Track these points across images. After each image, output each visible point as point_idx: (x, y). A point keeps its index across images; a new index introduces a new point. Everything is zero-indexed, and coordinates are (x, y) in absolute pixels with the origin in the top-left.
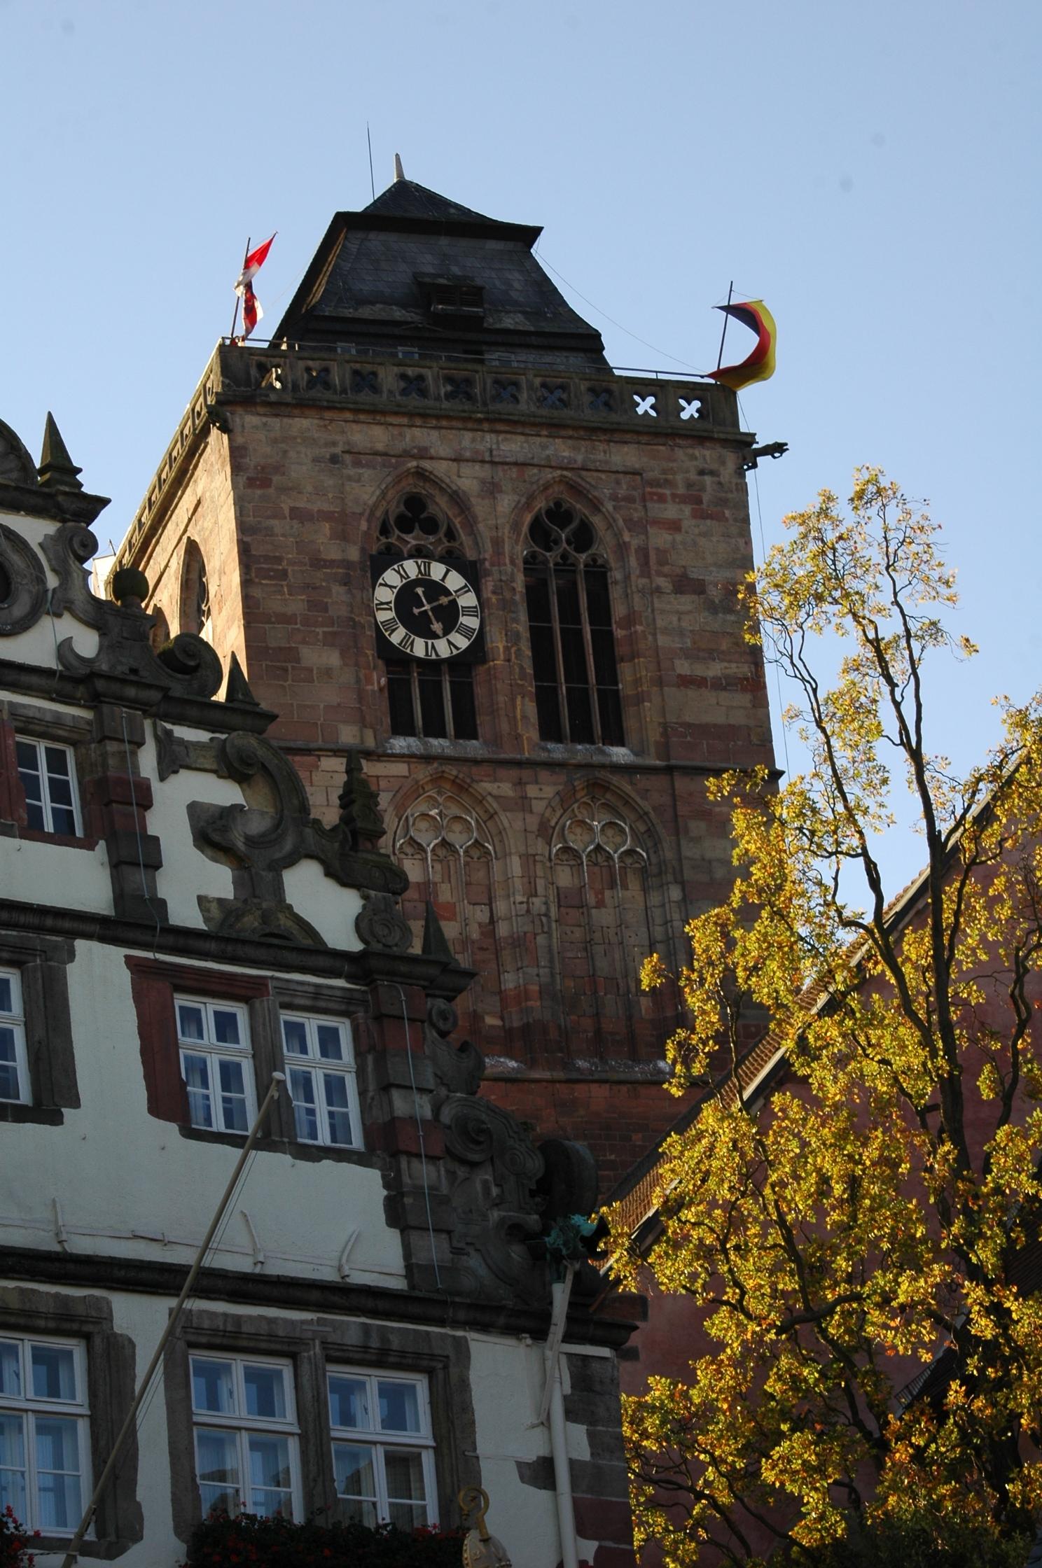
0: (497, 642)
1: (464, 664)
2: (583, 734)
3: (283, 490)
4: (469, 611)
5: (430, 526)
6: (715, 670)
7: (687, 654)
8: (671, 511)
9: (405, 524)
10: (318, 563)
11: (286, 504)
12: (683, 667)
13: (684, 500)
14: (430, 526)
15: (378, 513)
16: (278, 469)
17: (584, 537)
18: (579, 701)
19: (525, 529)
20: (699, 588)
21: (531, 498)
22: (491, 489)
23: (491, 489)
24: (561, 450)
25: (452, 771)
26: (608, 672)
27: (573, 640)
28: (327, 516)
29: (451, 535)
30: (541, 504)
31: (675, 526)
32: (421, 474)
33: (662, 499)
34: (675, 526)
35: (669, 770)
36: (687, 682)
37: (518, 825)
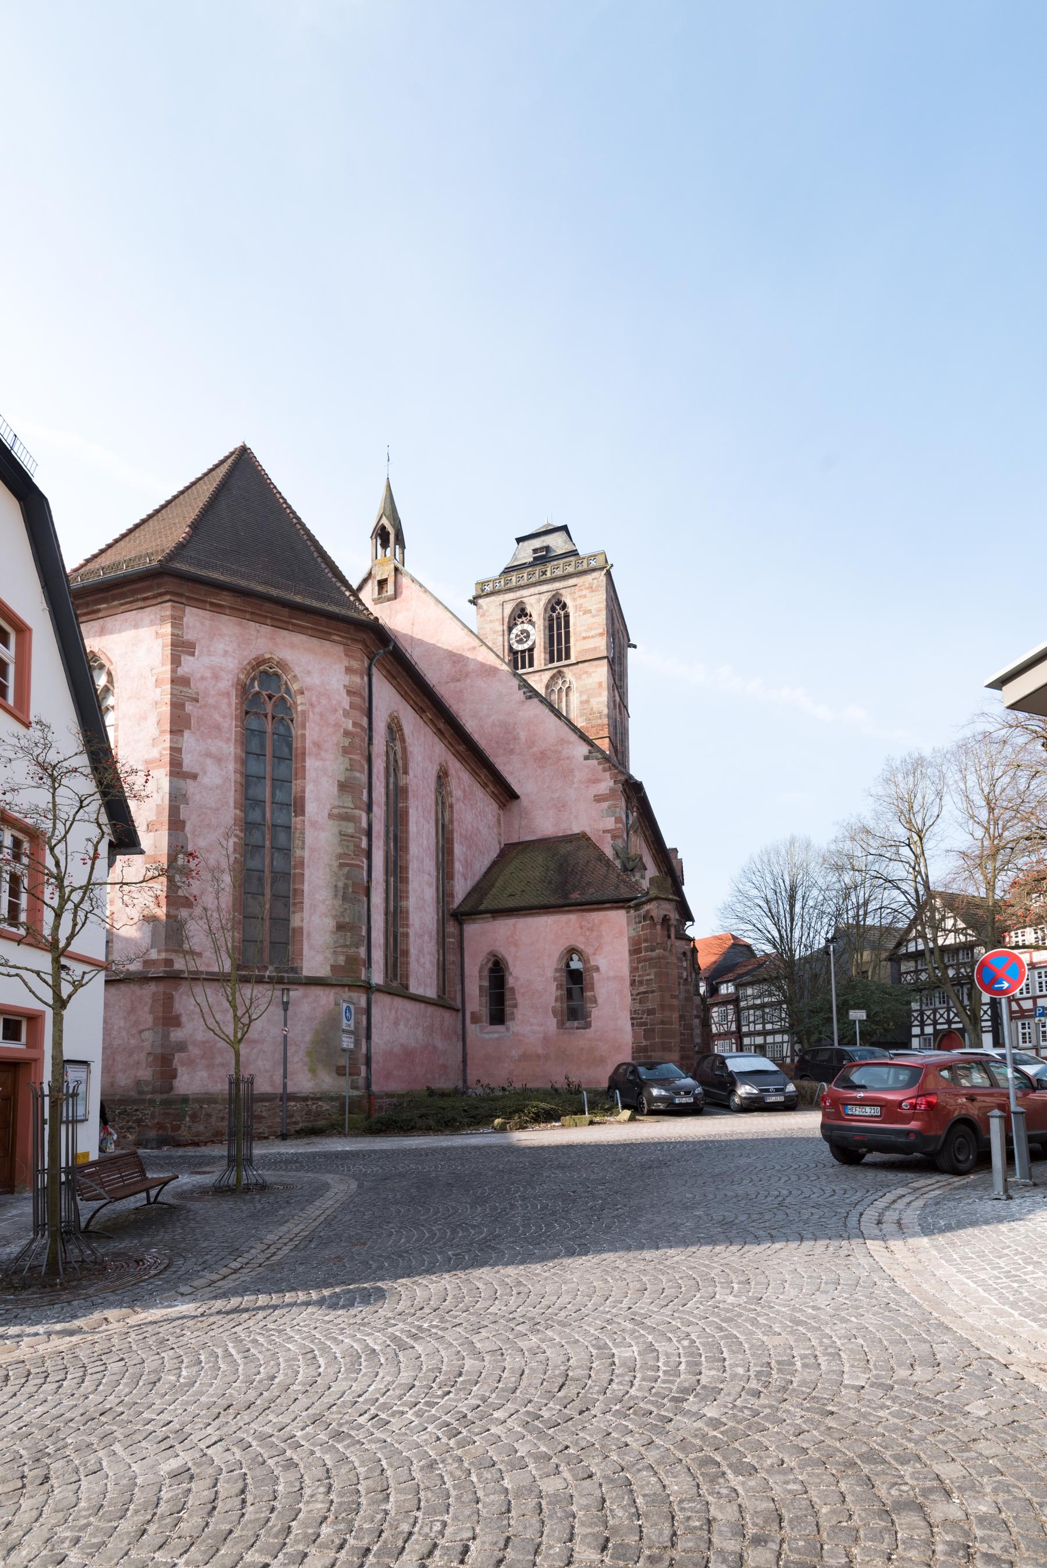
1: (531, 650)
5: (526, 615)
6: (593, 633)
7: (586, 631)
8: (584, 592)
9: (520, 617)
10: (495, 632)
12: (584, 635)
14: (526, 615)
17: (564, 606)
18: (559, 651)
20: (590, 611)
21: (550, 601)
22: (539, 601)
23: (539, 601)
24: (557, 585)
26: (568, 641)
27: (559, 635)
30: (553, 601)
31: (585, 596)
32: (522, 602)
34: (585, 596)
36: (584, 638)
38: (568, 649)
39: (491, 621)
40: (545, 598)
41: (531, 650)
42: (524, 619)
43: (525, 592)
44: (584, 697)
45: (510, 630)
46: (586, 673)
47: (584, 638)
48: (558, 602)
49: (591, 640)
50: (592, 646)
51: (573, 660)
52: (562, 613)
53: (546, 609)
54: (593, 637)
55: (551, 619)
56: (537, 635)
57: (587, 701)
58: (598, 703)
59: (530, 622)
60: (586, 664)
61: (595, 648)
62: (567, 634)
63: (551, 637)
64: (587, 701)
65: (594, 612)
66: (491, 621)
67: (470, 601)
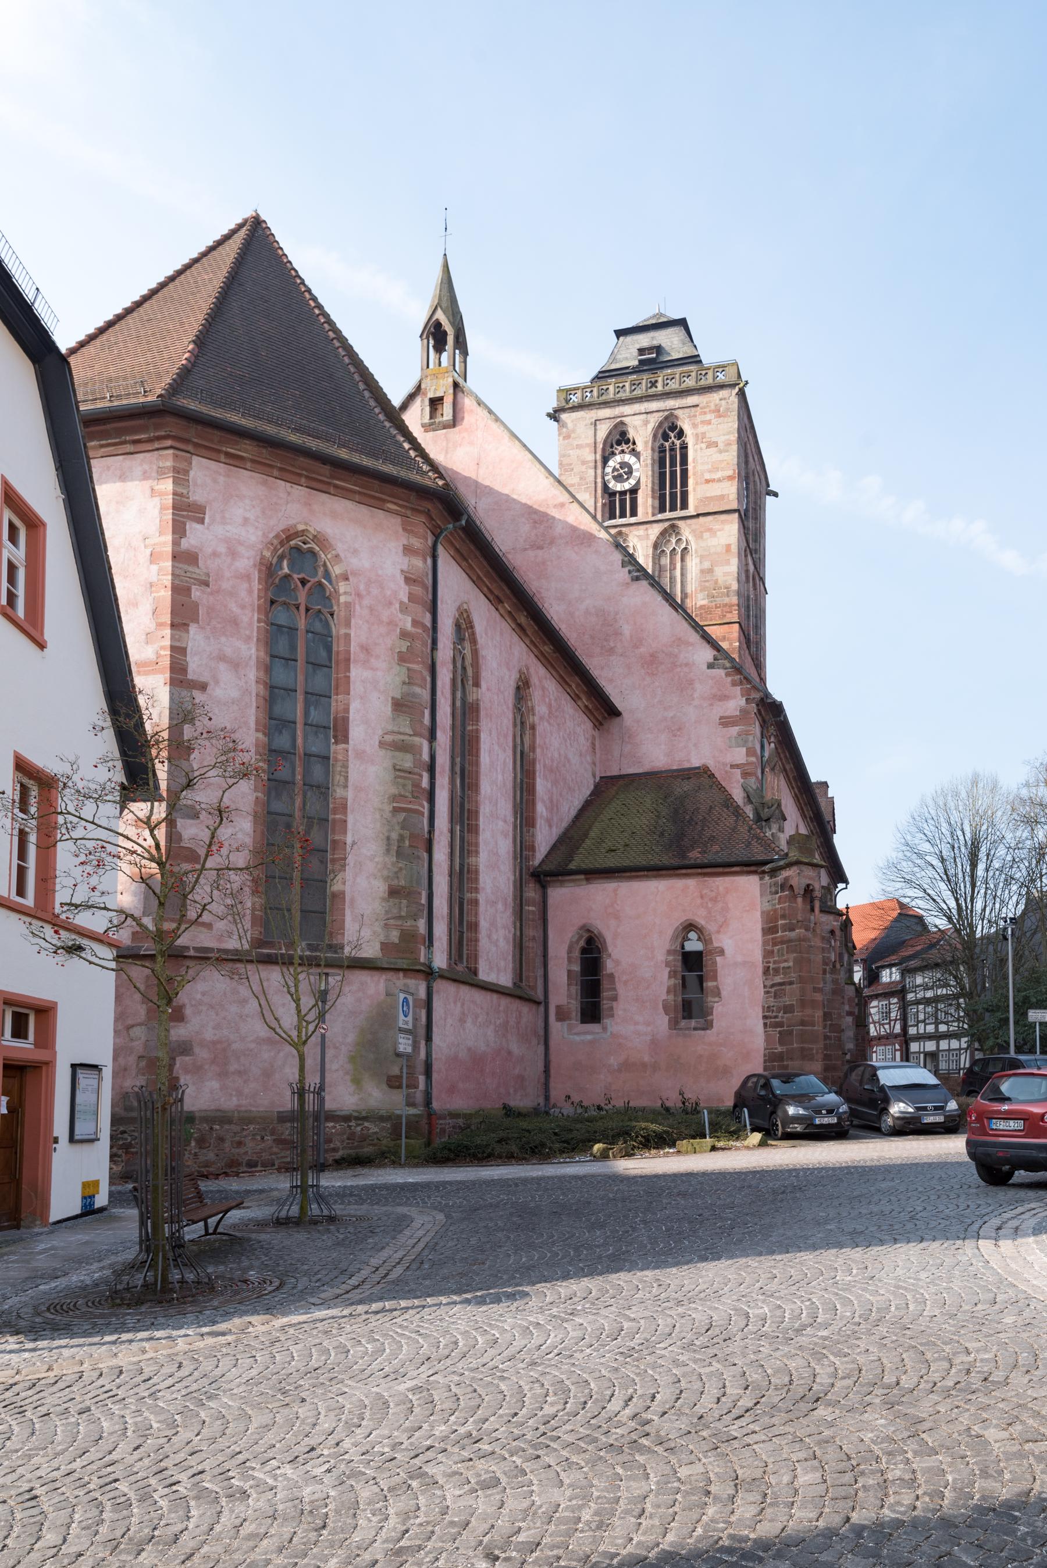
0: (643, 481)
1: (634, 491)
2: (673, 508)
3: (575, 438)
4: (638, 470)
5: (627, 442)
7: (710, 471)
8: (708, 417)
9: (619, 443)
10: (584, 463)
11: (576, 443)
12: (708, 476)
13: (714, 412)
14: (627, 442)
15: (609, 441)
16: (573, 431)
17: (681, 434)
18: (673, 496)
19: (660, 435)
20: (715, 444)
22: (646, 423)
23: (646, 423)
24: (671, 403)
25: (624, 529)
26: (684, 483)
27: (673, 474)
28: (588, 445)
29: (634, 443)
30: (666, 425)
31: (709, 422)
32: (622, 423)
33: (705, 413)
34: (709, 422)
35: (698, 515)
36: (708, 481)
37: (645, 545)
38: (685, 495)
39: (579, 447)
40: (654, 420)
41: (634, 491)
42: (624, 447)
43: (627, 409)
44: (707, 565)
45: (605, 460)
46: (710, 530)
47: (708, 481)
48: (673, 427)
49: (716, 485)
50: (718, 493)
51: (691, 510)
52: (678, 443)
53: (655, 436)
54: (719, 480)
55: (662, 450)
56: (643, 472)
57: (710, 571)
58: (726, 574)
59: (634, 452)
60: (710, 518)
61: (722, 497)
62: (685, 473)
63: (662, 475)
64: (710, 571)
65: (721, 446)
66: (579, 447)
67: (549, 415)
